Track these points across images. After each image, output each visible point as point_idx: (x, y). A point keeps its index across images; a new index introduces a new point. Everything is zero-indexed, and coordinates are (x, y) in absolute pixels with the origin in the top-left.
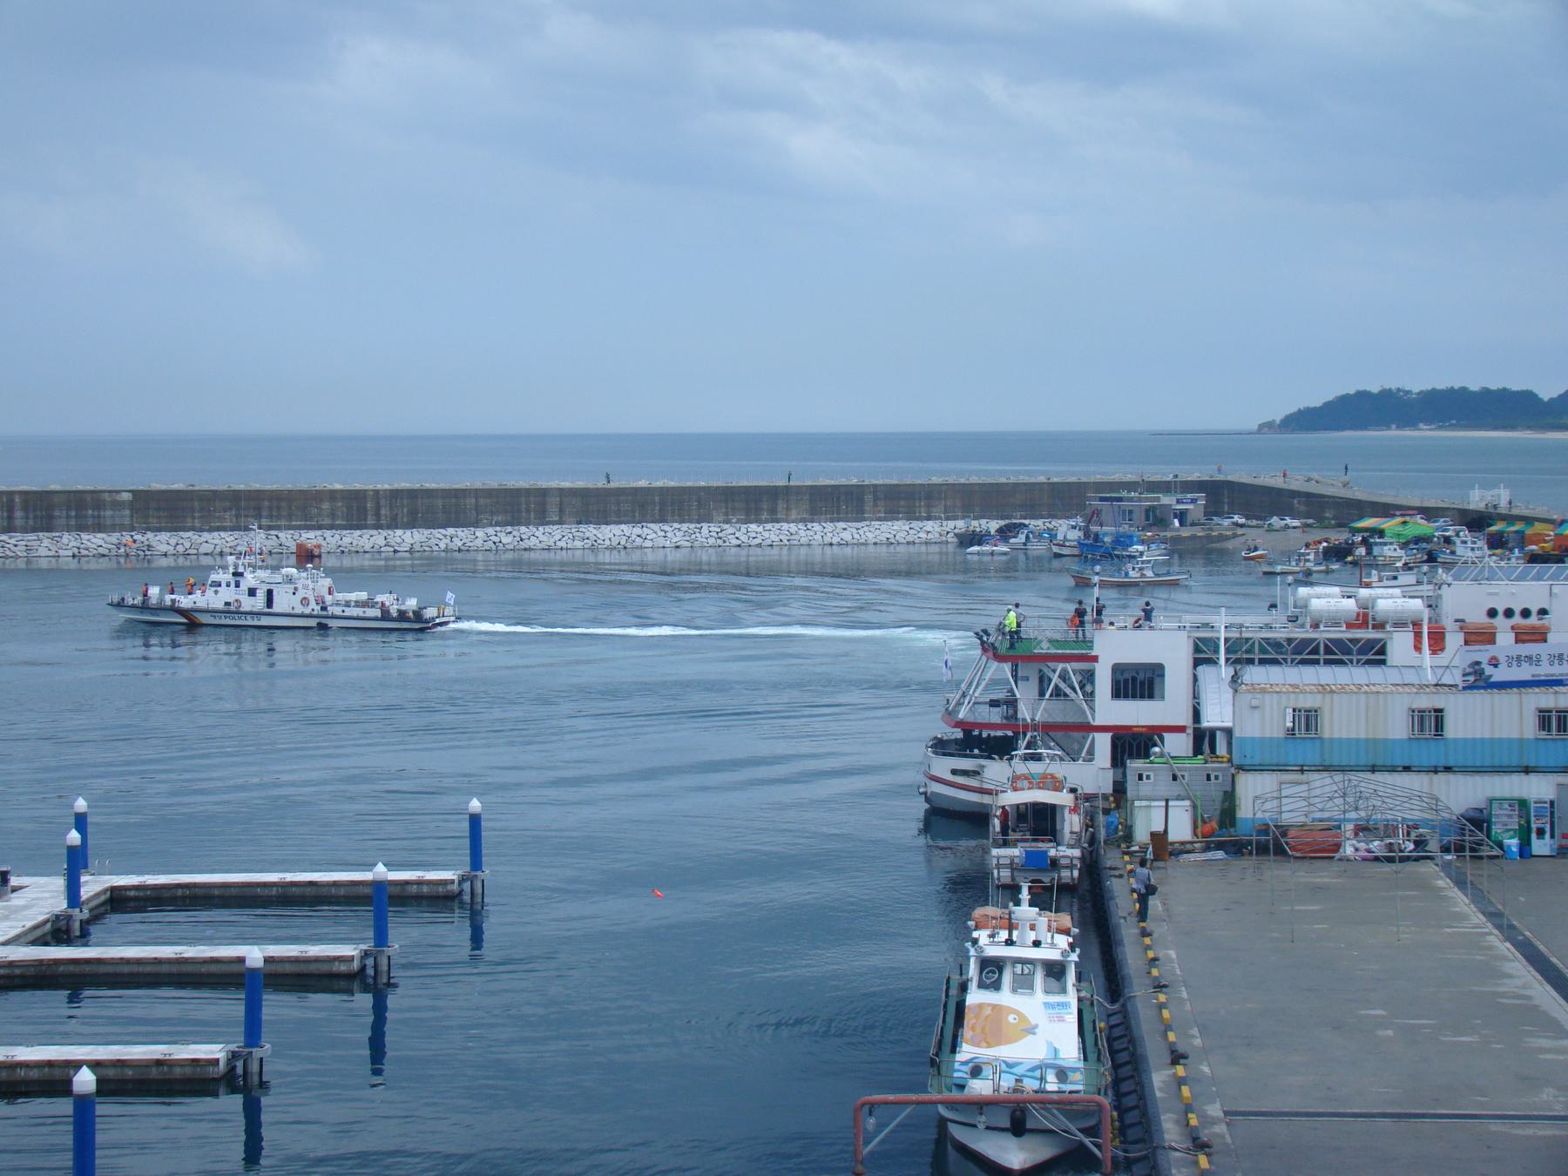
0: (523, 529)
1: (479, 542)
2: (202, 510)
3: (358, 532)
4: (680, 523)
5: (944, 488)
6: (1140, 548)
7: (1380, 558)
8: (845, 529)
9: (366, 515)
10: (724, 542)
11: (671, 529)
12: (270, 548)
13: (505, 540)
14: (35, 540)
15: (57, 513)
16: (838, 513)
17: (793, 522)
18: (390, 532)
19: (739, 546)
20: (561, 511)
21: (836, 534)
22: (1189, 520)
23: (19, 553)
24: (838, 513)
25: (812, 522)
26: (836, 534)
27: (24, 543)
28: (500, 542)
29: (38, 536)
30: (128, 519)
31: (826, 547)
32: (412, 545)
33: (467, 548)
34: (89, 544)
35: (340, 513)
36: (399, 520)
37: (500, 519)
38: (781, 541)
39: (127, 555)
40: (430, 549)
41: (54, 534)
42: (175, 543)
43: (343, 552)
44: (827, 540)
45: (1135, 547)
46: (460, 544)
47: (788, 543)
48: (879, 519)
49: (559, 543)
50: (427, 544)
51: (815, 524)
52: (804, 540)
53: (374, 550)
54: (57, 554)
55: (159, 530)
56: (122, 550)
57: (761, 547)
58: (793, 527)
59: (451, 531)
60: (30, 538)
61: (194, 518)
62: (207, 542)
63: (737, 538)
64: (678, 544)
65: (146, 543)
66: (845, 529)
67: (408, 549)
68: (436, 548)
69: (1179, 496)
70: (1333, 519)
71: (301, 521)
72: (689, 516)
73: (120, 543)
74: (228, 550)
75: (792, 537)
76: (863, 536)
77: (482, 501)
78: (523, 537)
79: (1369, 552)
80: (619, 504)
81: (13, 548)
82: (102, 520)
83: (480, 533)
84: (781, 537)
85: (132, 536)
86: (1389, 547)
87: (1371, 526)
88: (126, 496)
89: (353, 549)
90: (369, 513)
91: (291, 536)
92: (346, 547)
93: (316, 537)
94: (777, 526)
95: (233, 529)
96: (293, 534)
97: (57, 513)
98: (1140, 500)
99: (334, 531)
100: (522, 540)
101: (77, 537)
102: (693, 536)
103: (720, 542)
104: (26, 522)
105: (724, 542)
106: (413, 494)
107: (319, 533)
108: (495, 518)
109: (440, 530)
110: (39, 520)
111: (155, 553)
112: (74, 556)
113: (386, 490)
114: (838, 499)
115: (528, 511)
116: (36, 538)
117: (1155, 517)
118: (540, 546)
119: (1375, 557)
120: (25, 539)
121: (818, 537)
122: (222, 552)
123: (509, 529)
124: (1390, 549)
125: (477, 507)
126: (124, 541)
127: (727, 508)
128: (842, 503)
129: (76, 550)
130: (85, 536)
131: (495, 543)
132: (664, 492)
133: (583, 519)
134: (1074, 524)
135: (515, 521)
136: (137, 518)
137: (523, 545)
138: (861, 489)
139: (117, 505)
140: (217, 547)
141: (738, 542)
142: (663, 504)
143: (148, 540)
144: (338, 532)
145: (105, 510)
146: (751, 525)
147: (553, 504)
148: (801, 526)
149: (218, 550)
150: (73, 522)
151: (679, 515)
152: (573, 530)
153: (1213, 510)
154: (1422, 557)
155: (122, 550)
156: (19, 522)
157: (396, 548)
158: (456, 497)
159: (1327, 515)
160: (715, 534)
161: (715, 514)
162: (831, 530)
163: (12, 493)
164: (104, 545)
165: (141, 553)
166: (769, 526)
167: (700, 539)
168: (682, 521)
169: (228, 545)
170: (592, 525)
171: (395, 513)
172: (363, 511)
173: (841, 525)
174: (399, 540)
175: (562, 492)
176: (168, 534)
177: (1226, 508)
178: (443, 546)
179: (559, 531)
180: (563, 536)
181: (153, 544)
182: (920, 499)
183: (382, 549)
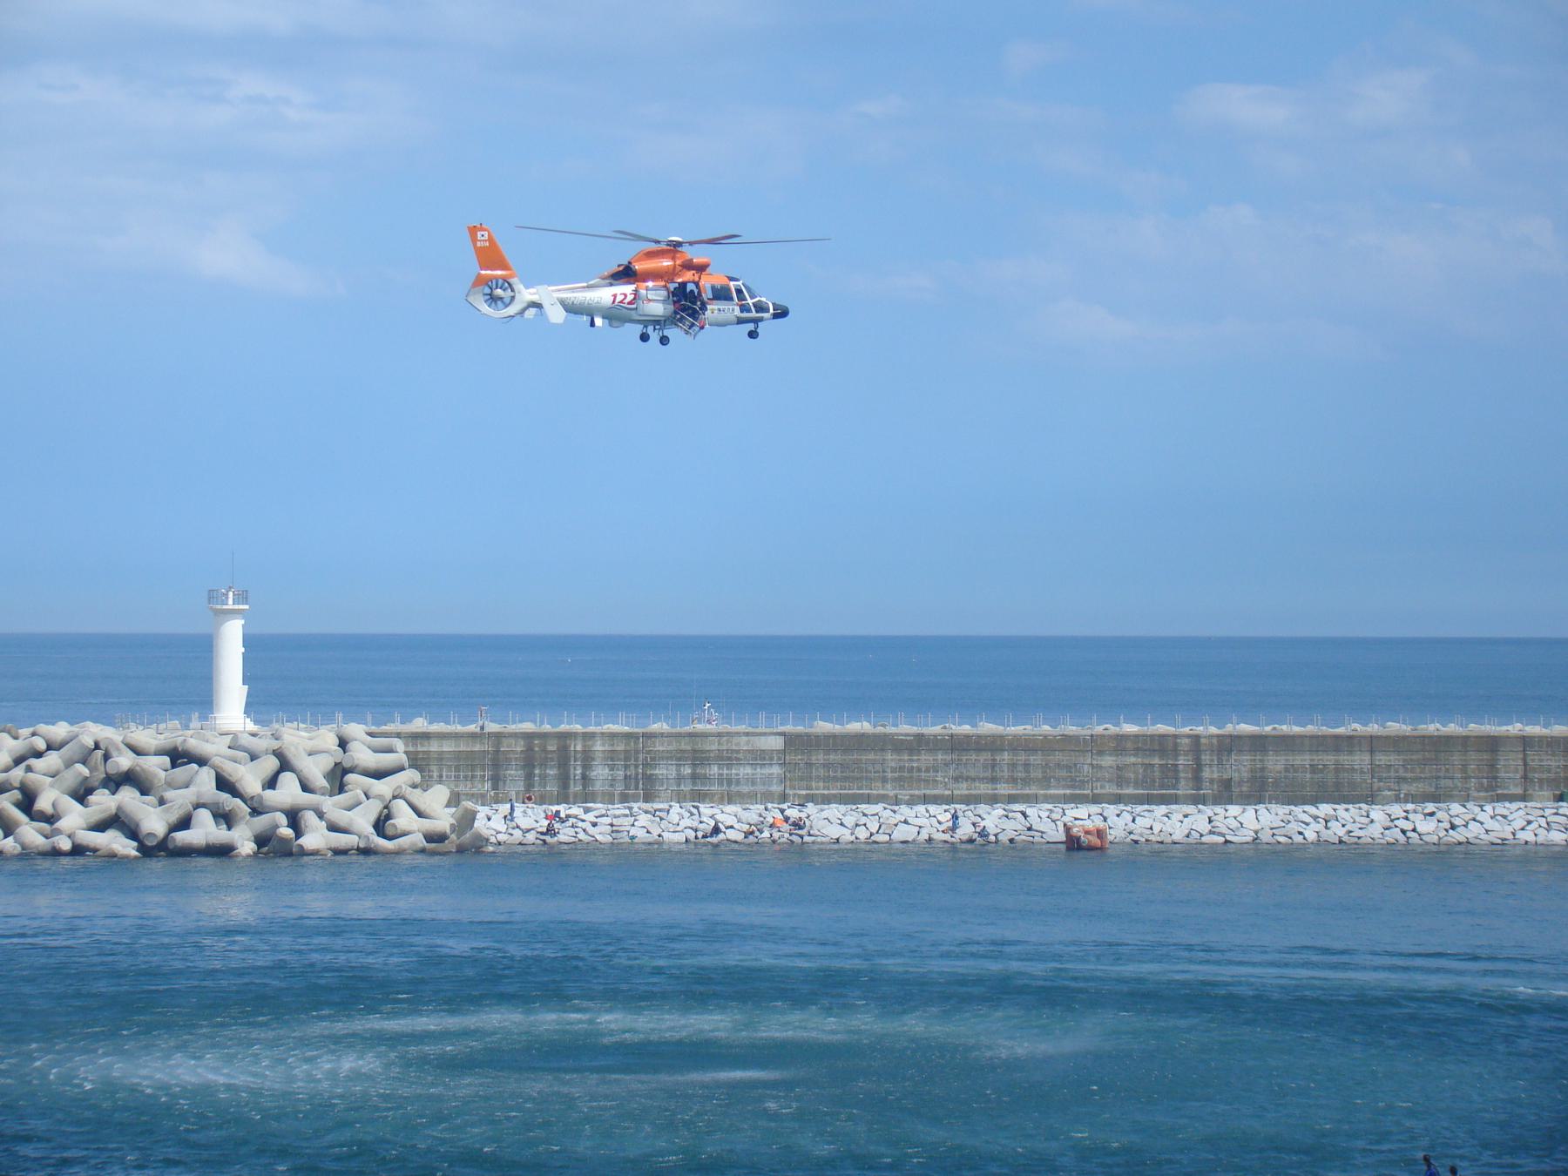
0: (1456, 808)
1: (1375, 831)
3: (1163, 809)
9: (1177, 779)
12: (1012, 835)
13: (1426, 826)
14: (626, 816)
15: (659, 771)
18: (1219, 809)
23: (599, 837)
27: (607, 820)
32: (1256, 832)
35: (1132, 776)
36: (1236, 790)
42: (853, 823)
43: (1136, 842)
46: (1341, 832)
49: (1523, 836)
50: (1282, 831)
53: (1191, 840)
55: (827, 800)
56: (766, 834)
59: (1325, 809)
60: (617, 812)
61: (884, 780)
62: (906, 822)
67: (1249, 839)
71: (1064, 787)
77: (1382, 759)
78: (1457, 821)
81: (591, 830)
83: (1377, 813)
85: (782, 811)
88: (776, 743)
89: (1153, 838)
90: (1182, 775)
91: (1048, 813)
92: (1141, 835)
93: (1089, 816)
96: (1051, 811)
97: (659, 771)
99: (1122, 807)
100: (1453, 827)
101: (695, 811)
107: (1094, 809)
108: (1405, 788)
109: (1308, 808)
110: (633, 781)
111: (819, 839)
113: (1211, 736)
115: (1467, 778)
116: (627, 812)
123: (1430, 807)
125: (1374, 769)
126: (771, 820)
129: (691, 834)
130: (705, 809)
131: (1403, 832)
137: (1456, 836)
139: (760, 757)
143: (807, 818)
144: (1129, 808)
147: (1510, 764)
149: (924, 836)
150: (686, 787)
152: (1548, 812)
155: (766, 834)
156: (598, 787)
157: (1228, 838)
163: (592, 736)
164: (735, 826)
165: (794, 838)
169: (941, 828)
172: (1170, 774)
174: (1234, 824)
175: (1526, 742)
176: (843, 808)
178: (1311, 835)
179: (1521, 813)
180: (1529, 822)
183: (1204, 839)
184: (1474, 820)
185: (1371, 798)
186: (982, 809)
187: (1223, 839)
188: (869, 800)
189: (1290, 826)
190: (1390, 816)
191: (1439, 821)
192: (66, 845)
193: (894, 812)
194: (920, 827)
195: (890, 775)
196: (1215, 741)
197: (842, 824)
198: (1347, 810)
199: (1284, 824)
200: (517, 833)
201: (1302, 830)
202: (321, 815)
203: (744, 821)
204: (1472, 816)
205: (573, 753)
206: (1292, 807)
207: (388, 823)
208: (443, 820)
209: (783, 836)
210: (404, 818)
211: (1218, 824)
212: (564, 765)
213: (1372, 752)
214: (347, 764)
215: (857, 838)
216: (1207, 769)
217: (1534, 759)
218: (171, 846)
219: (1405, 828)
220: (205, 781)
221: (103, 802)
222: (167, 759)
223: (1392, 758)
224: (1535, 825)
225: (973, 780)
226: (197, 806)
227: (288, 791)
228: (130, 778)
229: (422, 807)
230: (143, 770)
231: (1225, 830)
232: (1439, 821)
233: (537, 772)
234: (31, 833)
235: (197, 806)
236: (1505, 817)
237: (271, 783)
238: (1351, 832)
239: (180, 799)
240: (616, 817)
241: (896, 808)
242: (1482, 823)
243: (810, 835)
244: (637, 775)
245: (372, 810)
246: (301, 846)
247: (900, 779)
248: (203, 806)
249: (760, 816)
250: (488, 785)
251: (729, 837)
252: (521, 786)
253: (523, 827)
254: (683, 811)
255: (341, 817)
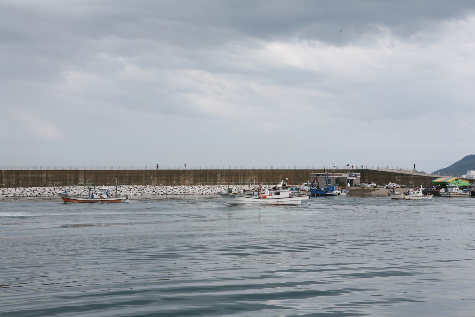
0: (67, 187)
1: (46, 193)
4: (137, 185)
5: (251, 171)
6: (338, 192)
7: (452, 193)
8: (208, 188)
10: (156, 193)
11: (133, 188)
16: (206, 182)
17: (186, 185)
18: (6, 189)
19: (163, 195)
20: (85, 180)
21: (205, 190)
22: (354, 184)
24: (206, 182)
25: (195, 185)
26: (205, 190)
28: (56, 193)
31: (200, 195)
32: (15, 194)
33: (40, 195)
36: (11, 184)
37: (57, 183)
38: (181, 193)
40: (23, 196)
44: (201, 192)
45: (335, 191)
46: (37, 193)
47: (183, 194)
48: (223, 184)
49: (83, 194)
50: (22, 194)
51: (196, 186)
52: (191, 193)
57: (172, 195)
58: (186, 187)
59: (34, 188)
63: (162, 191)
64: (136, 194)
66: (208, 188)
67: (13, 196)
68: (26, 195)
69: (350, 174)
70: (413, 184)
72: (142, 182)
75: (186, 191)
76: (216, 191)
77: (49, 175)
78: (67, 191)
79: (446, 191)
80: (111, 177)
83: (47, 189)
84: (181, 191)
86: (455, 188)
87: (442, 181)
94: (179, 186)
98: (333, 175)
102: (143, 191)
103: (154, 193)
105: (156, 193)
106: (18, 172)
108: (55, 183)
109: (29, 188)
114: (206, 176)
115: (70, 180)
117: (340, 182)
118: (74, 194)
119: (449, 193)
121: (197, 191)
123: (61, 187)
124: (455, 190)
125: (47, 178)
127: (158, 179)
128: (207, 177)
131: (53, 193)
132: (131, 172)
133: (95, 183)
134: (306, 183)
135: (64, 184)
138: (216, 171)
141: (162, 193)
142: (130, 177)
146: (168, 186)
147: (81, 176)
148: (189, 187)
151: (137, 182)
153: (363, 180)
154: (469, 194)
157: (7, 195)
158: (37, 174)
159: (410, 183)
160: (152, 190)
161: (153, 181)
162: (202, 188)
166: (176, 187)
167: (145, 192)
168: (139, 185)
170: (98, 186)
171: (9, 180)
173: (207, 186)
174: (9, 192)
175: (85, 172)
177: (367, 181)
178: (29, 194)
179: (83, 188)
180: (85, 191)
182: (240, 176)
184: (72, 190)
185: (46, 185)
187: (5, 196)
189: (24, 192)
190: (50, 189)
191: (62, 191)
196: (6, 171)
198: (39, 188)
199: (22, 192)
201: (27, 193)
204: (71, 189)
206: (26, 188)
211: (5, 192)
213: (47, 174)
216: (4, 179)
217: (87, 175)
219: (54, 192)
223: (52, 175)
224: (86, 191)
231: (7, 194)
232: (62, 191)
236: (79, 189)
238: (40, 193)
242: (73, 191)
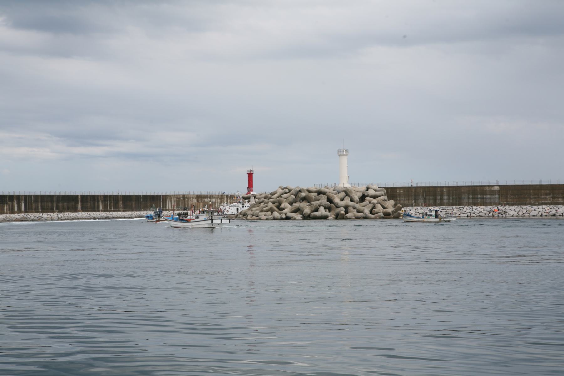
2: (535, 194)
14: (451, 209)
15: (463, 197)
27: (445, 210)
29: (452, 207)
30: (497, 199)
34: (476, 211)
39: (493, 216)
41: (460, 207)
42: (518, 211)
54: (459, 216)
55: (513, 205)
56: (491, 214)
60: (448, 208)
61: (530, 199)
62: (535, 210)
65: (504, 210)
73: (491, 211)
74: (545, 214)
82: (485, 200)
85: (498, 207)
88: (497, 188)
95: (550, 204)
97: (463, 197)
101: (471, 208)
104: (449, 201)
110: (455, 200)
112: (467, 216)
116: (451, 208)
120: (446, 208)
122: (542, 215)
126: (493, 210)
129: (469, 214)
130: (474, 207)
136: (502, 199)
139: (492, 193)
140: (540, 212)
143: (505, 209)
145: (486, 195)
149: (540, 214)
150: (471, 201)
155: (491, 214)
156: (445, 201)
163: (442, 188)
164: (483, 212)
165: (500, 215)
169: (545, 212)
176: (516, 206)
181: (507, 211)
186: (559, 206)
188: (525, 204)
192: (284, 216)
193: (532, 207)
194: (539, 211)
195: (532, 197)
197: (515, 211)
200: (418, 214)
202: (354, 208)
203: (485, 210)
205: (437, 192)
207: (374, 209)
208: (390, 210)
209: (496, 214)
210: (379, 208)
212: (435, 195)
214: (366, 194)
215: (519, 215)
218: (311, 216)
220: (323, 200)
221: (296, 205)
222: (316, 194)
225: (558, 198)
226: (320, 206)
227: (347, 201)
228: (304, 199)
229: (385, 206)
230: (308, 196)
233: (427, 197)
234: (276, 214)
235: (320, 206)
237: (342, 200)
239: (315, 203)
240: (448, 209)
241: (533, 206)
243: (505, 214)
244: (456, 198)
245: (371, 206)
246: (346, 216)
247: (535, 198)
248: (322, 206)
249: (491, 209)
250: (413, 202)
251: (480, 215)
252: (423, 201)
253: (419, 212)
254: (468, 208)
255: (361, 208)
